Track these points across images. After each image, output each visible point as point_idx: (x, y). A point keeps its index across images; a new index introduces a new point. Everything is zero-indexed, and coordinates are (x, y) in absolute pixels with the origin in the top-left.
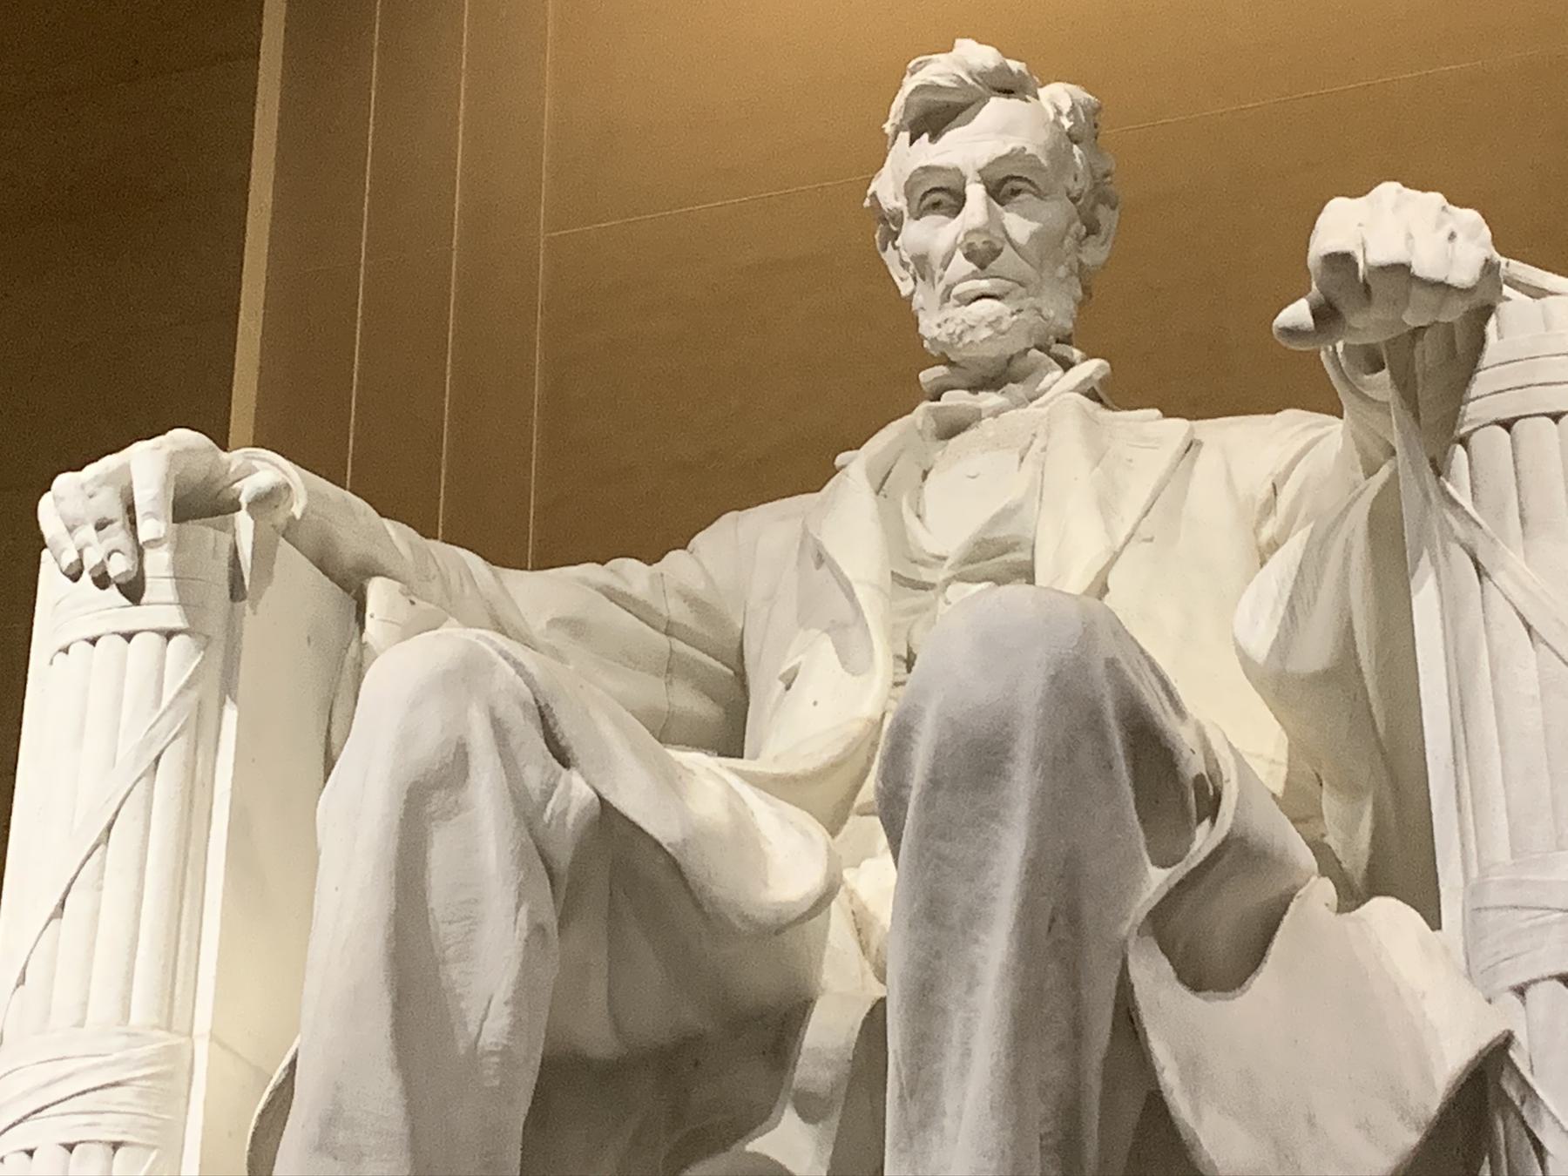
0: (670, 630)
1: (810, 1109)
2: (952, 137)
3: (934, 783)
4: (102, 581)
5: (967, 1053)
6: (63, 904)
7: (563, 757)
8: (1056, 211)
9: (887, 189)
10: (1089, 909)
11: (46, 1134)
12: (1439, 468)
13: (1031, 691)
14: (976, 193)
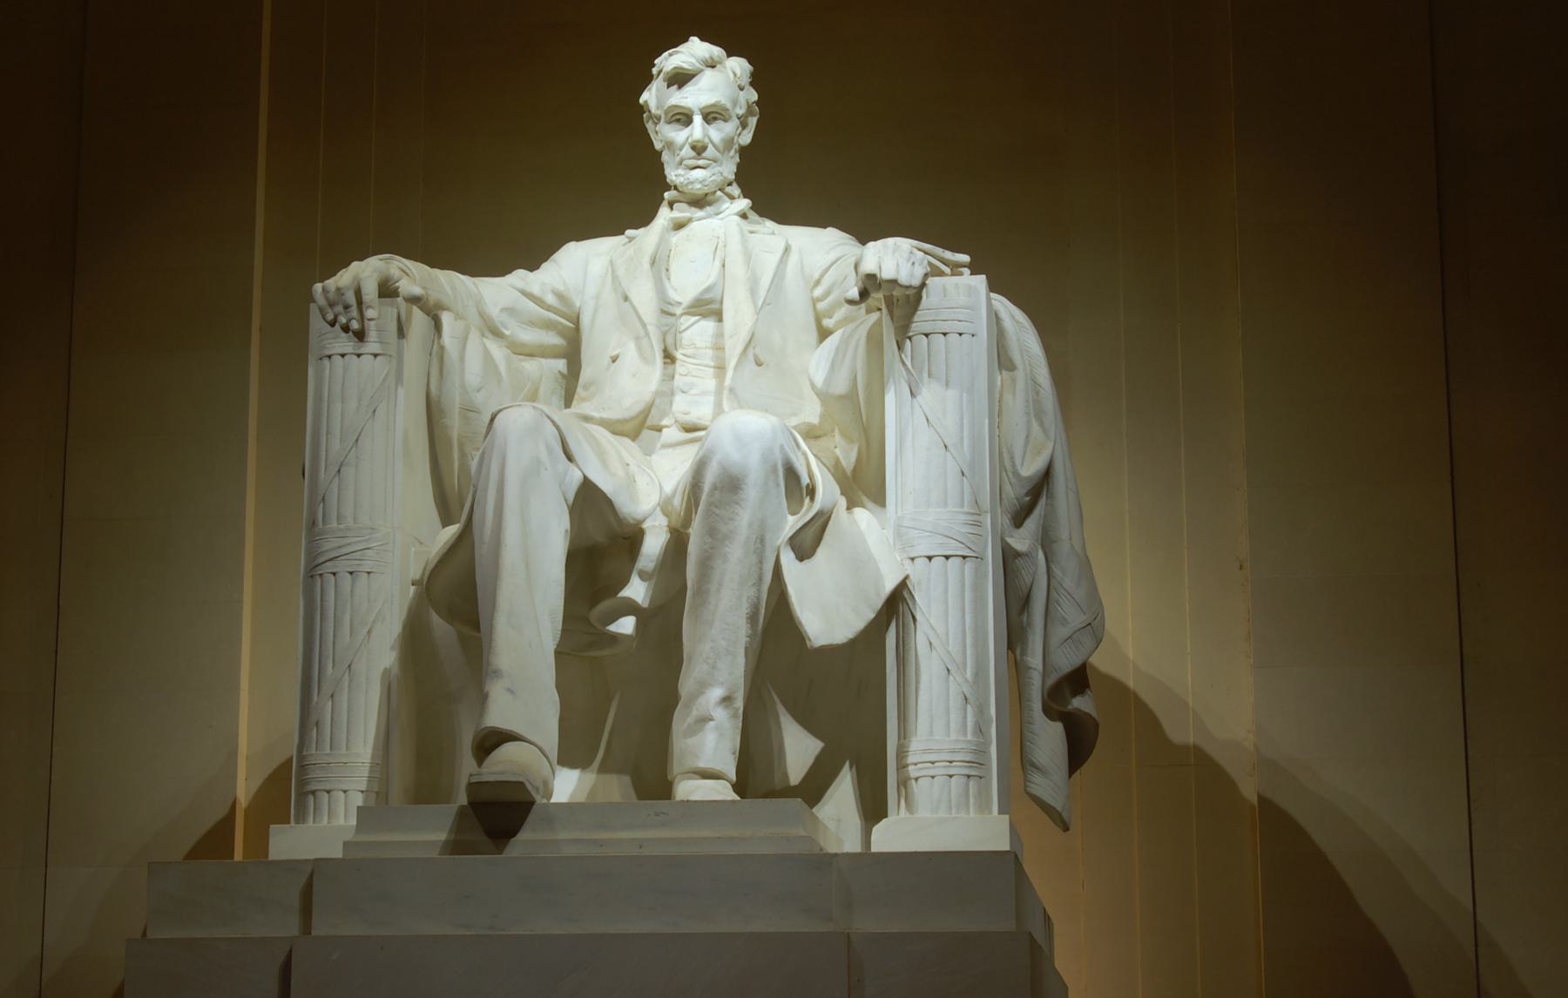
0: (549, 308)
1: (643, 576)
2: (689, 89)
4: (346, 329)
5: (720, 584)
7: (570, 458)
9: (649, 97)
10: (768, 536)
11: (342, 566)
12: (900, 347)
14: (698, 119)
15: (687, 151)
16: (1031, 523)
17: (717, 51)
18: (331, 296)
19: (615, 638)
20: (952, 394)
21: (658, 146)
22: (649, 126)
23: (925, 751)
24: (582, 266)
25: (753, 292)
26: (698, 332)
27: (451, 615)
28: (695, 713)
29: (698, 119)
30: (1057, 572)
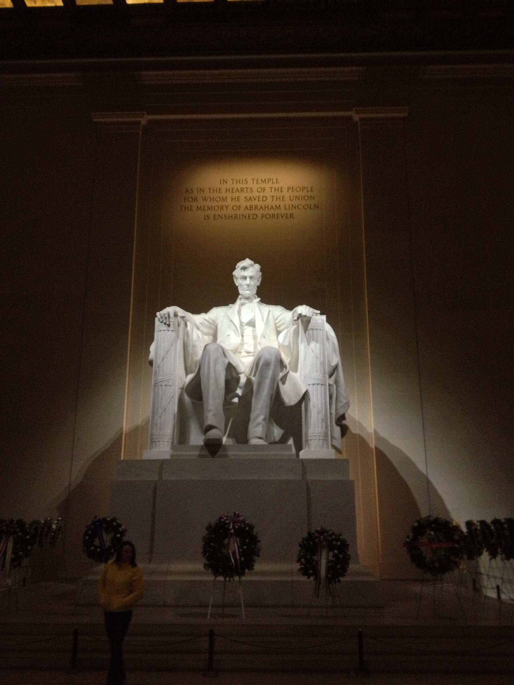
0: (210, 323)
1: (241, 388)
3: (263, 365)
4: (165, 324)
6: (163, 360)
8: (256, 281)
11: (163, 384)
13: (273, 359)
14: (248, 279)
15: (245, 287)
16: (333, 377)
17: (252, 262)
18: (162, 315)
19: (233, 403)
20: (318, 345)
21: (237, 285)
22: (235, 280)
23: (313, 433)
25: (263, 320)
26: (248, 330)
27: (190, 396)
28: (256, 422)
30: (339, 389)
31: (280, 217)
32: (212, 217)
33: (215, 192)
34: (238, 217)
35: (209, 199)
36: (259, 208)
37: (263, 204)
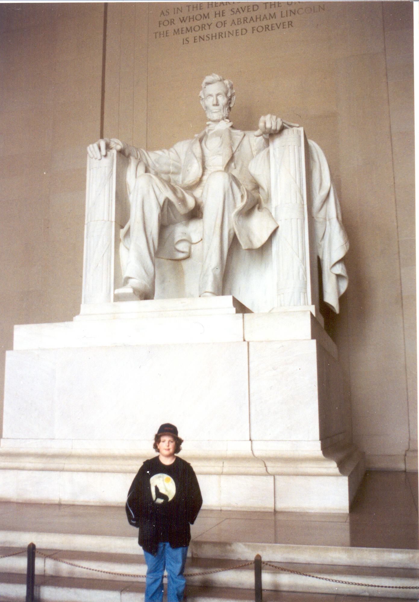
24: (182, 147)
29: (215, 96)
31: (276, 27)
32: (191, 40)
33: (195, 9)
34: (223, 35)
35: (188, 18)
36: (248, 20)
37: (253, 14)
